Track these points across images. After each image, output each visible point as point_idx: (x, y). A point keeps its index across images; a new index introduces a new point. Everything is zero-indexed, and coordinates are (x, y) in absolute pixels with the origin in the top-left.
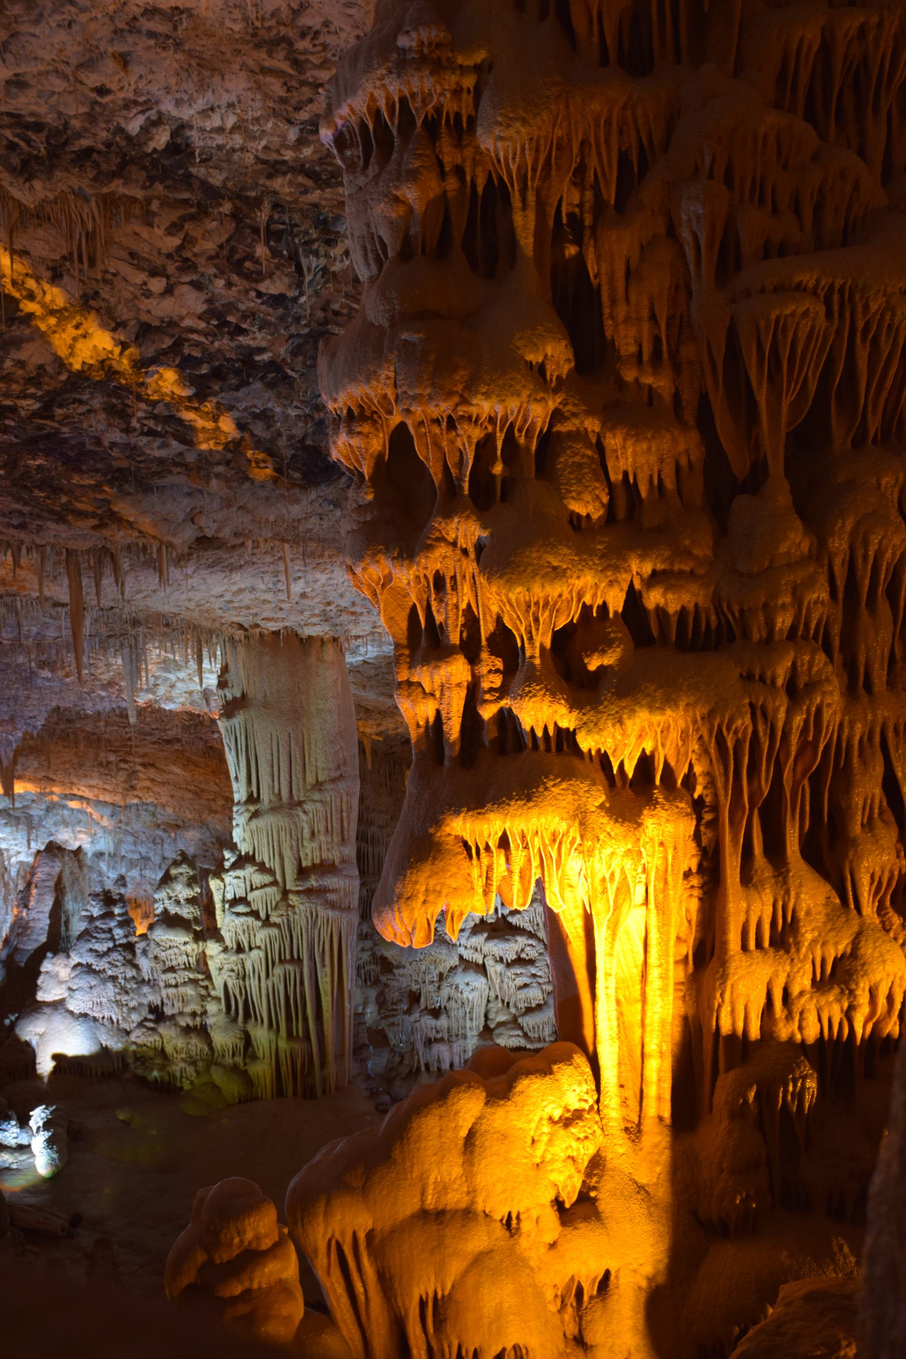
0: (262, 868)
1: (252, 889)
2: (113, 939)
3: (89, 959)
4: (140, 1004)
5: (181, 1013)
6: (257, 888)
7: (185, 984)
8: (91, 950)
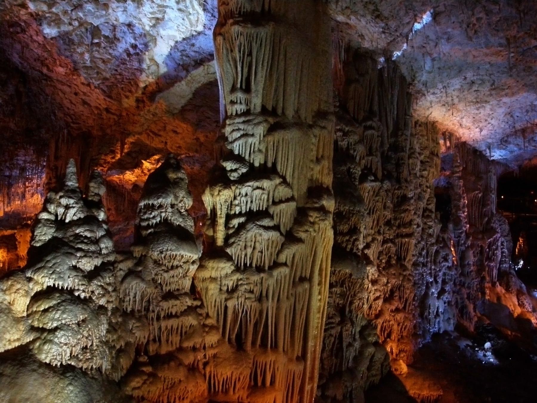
0: (284, 182)
1: (275, 203)
2: (99, 253)
3: (69, 282)
4: (127, 344)
5: (181, 349)
6: (281, 202)
7: (185, 313)
8: (75, 268)
